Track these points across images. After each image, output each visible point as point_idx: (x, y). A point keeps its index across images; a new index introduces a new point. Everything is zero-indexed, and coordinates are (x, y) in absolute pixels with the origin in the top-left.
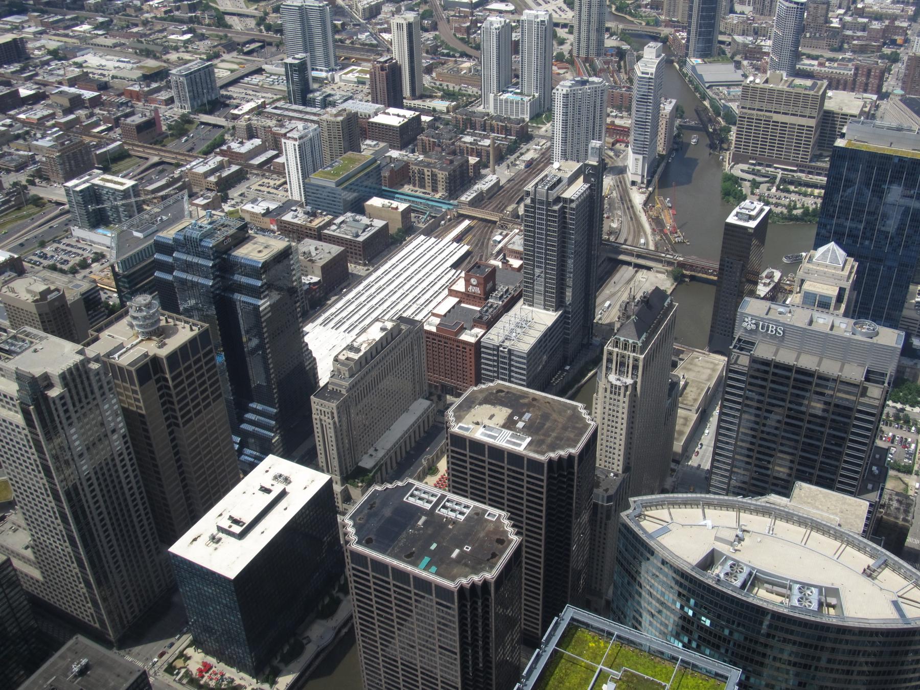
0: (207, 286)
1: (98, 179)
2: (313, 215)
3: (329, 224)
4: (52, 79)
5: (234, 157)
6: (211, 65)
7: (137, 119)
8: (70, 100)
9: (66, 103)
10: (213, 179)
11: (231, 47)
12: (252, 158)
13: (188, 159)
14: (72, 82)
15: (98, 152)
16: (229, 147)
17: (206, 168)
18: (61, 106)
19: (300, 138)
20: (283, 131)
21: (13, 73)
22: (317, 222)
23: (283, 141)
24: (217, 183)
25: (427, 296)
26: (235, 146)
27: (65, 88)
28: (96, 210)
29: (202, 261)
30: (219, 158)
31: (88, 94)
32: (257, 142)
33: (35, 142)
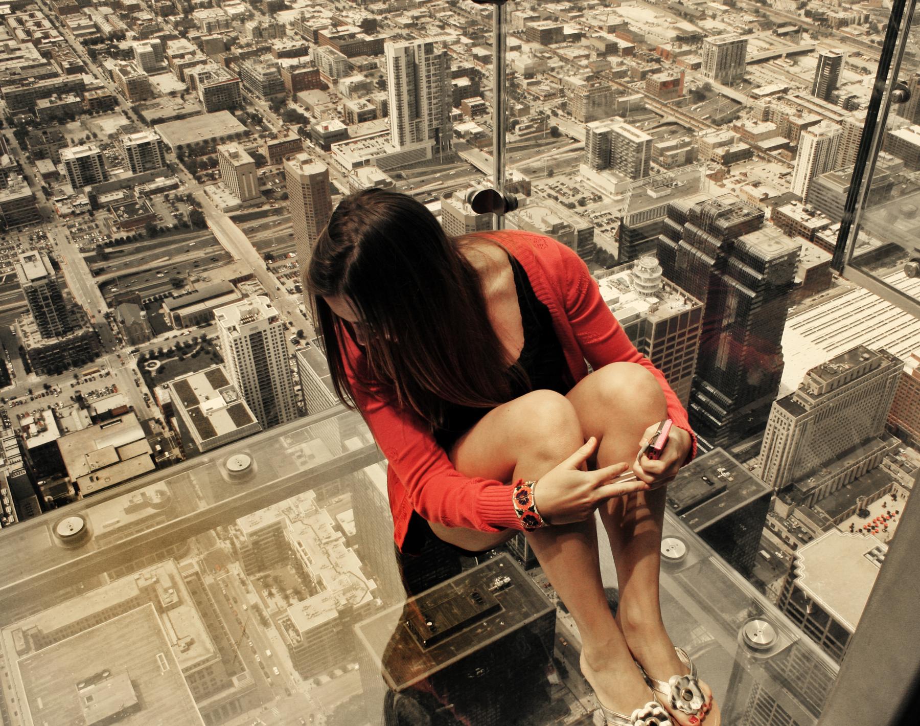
0: (704, 265)
1: (618, 125)
2: (812, 214)
3: (824, 228)
4: (595, 23)
5: (746, 136)
6: (746, 41)
7: (663, 77)
8: (607, 45)
9: (602, 47)
10: (721, 151)
11: (767, 25)
12: (762, 140)
13: (701, 126)
14: (612, 29)
15: (621, 100)
16: (743, 125)
17: (718, 140)
18: (598, 50)
19: (821, 135)
20: (800, 122)
21: (562, 10)
22: (814, 223)
23: (803, 133)
24: (723, 157)
25: (906, 331)
26: (749, 126)
27: (604, 34)
28: (606, 154)
29: (711, 240)
30: (732, 133)
31: (623, 44)
32: (771, 126)
33: (567, 78)
